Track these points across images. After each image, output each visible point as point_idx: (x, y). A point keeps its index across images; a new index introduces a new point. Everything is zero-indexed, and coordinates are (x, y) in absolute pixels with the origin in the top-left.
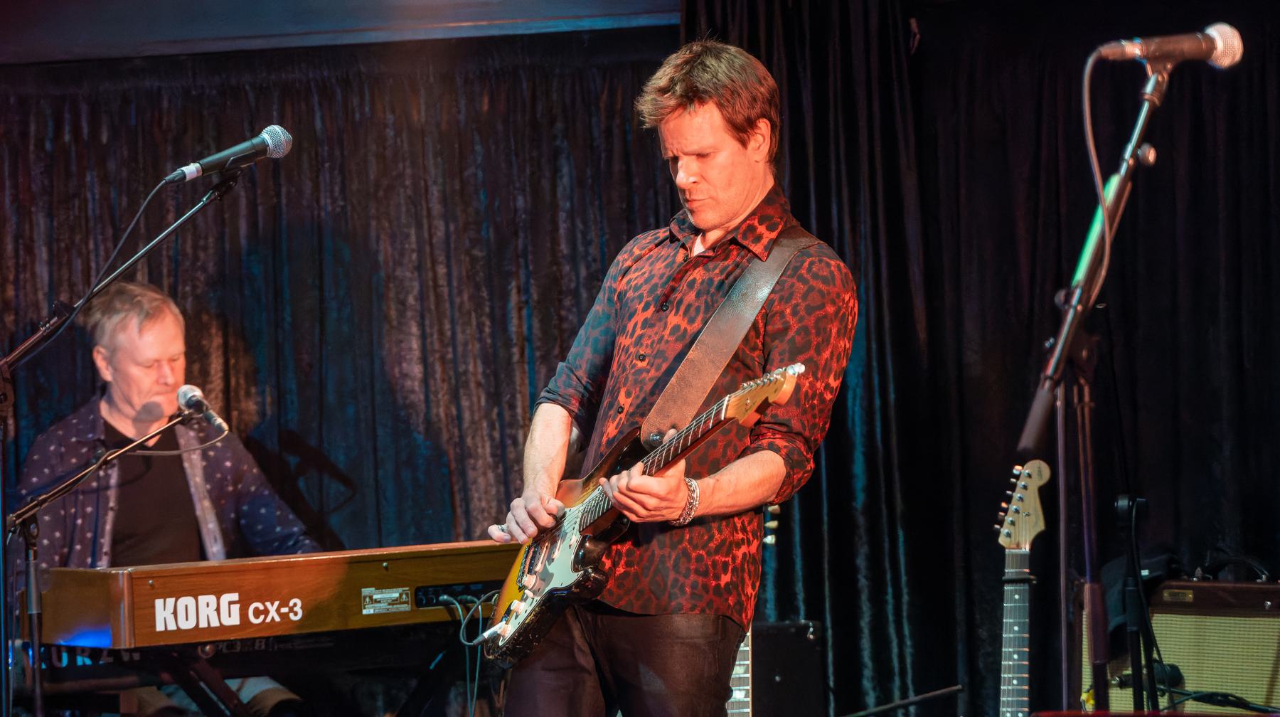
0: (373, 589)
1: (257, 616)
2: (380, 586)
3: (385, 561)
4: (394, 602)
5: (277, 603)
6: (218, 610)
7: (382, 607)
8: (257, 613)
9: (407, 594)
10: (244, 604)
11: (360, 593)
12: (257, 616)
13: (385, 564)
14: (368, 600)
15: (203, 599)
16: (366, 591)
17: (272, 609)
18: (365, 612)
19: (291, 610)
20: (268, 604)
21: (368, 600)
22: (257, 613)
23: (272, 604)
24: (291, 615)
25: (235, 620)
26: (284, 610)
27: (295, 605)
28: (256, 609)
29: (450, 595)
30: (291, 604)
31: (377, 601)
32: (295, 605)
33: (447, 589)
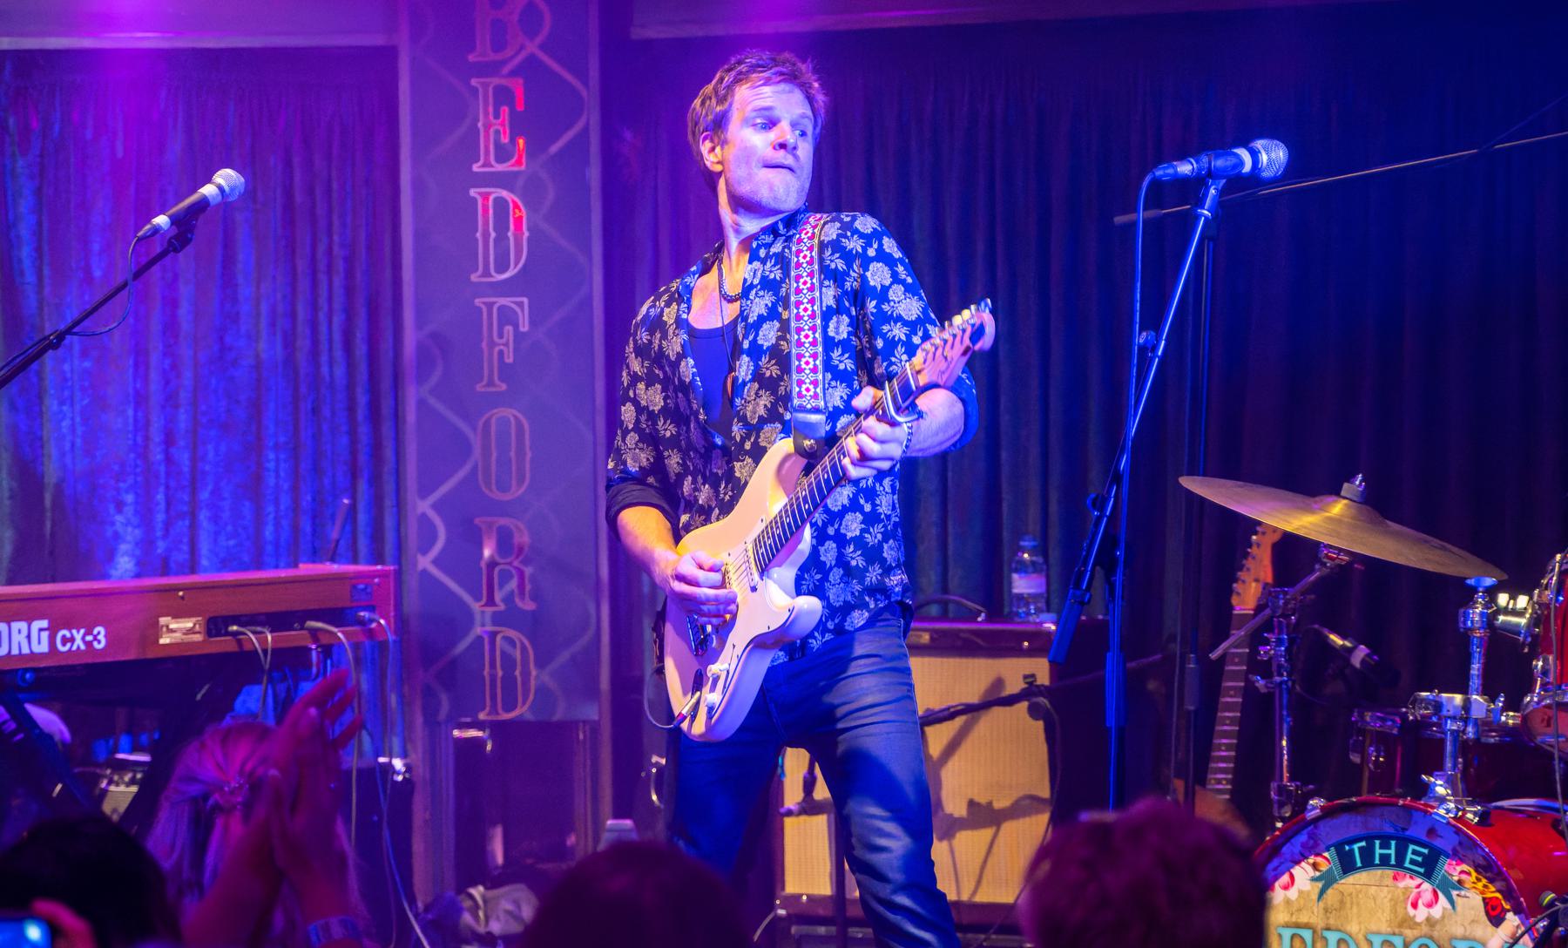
0: (169, 618)
1: (64, 644)
2: (177, 615)
3: (181, 590)
4: (190, 631)
5: (82, 631)
6: (29, 637)
7: (178, 636)
8: (65, 641)
9: (200, 624)
11: (158, 622)
12: (64, 644)
13: (181, 593)
14: (164, 629)
15: (16, 626)
16: (163, 620)
17: (78, 635)
18: (162, 641)
19: (95, 638)
20: (74, 632)
21: (164, 629)
22: (65, 641)
23: (78, 632)
24: (95, 644)
25: (44, 648)
26: (89, 638)
27: (99, 633)
28: (64, 636)
29: (239, 625)
30: (95, 632)
31: (172, 631)
32: (99, 633)
33: (236, 620)
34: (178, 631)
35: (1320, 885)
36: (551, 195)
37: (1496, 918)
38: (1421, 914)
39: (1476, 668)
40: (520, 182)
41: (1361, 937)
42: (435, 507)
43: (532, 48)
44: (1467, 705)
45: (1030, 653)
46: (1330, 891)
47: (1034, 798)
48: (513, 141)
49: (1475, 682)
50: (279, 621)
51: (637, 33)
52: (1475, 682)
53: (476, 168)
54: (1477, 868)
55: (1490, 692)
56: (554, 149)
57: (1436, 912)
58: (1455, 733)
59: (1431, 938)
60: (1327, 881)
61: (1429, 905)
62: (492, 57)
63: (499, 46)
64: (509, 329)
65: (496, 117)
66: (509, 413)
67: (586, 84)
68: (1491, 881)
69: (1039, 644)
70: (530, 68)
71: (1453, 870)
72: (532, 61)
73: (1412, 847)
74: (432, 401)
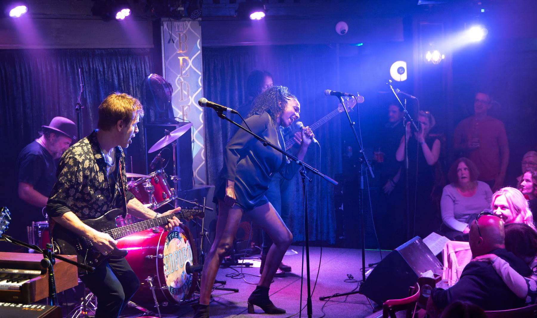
35: (167, 245)
37: (186, 242)
38: (178, 246)
41: (173, 254)
46: (169, 246)
54: (183, 233)
57: (180, 244)
59: (180, 250)
60: (168, 244)
61: (179, 243)
71: (181, 235)
73: (176, 233)
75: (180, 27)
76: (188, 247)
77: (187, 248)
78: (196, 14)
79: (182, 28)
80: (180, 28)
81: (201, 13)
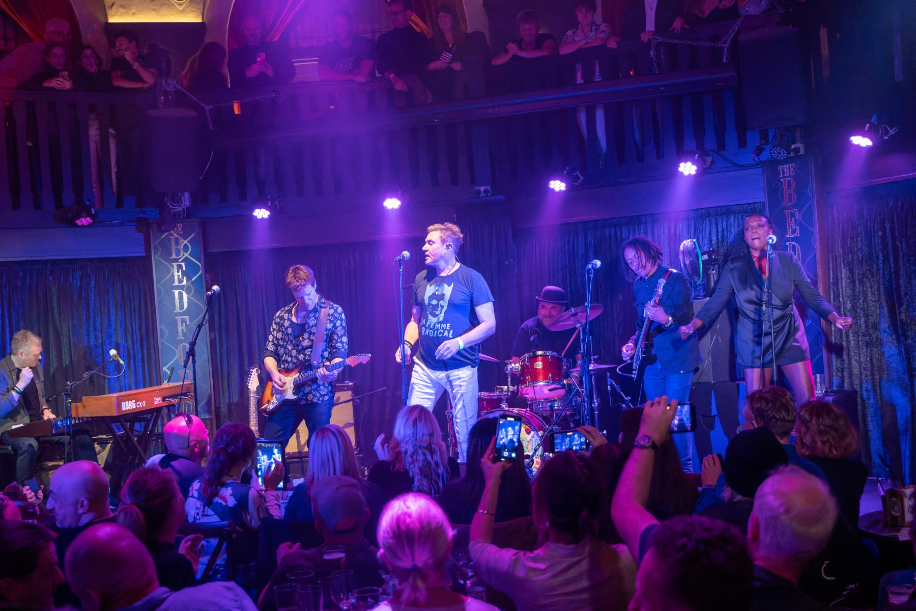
4: (160, 401)
8: (139, 405)
10: (136, 402)
16: (155, 398)
18: (155, 403)
22: (139, 405)
33: (168, 397)
34: (158, 401)
36: (193, 291)
39: (509, 380)
40: (185, 289)
42: (167, 368)
43: (187, 255)
44: (508, 388)
45: (347, 390)
47: (348, 423)
48: (183, 278)
49: (509, 383)
50: (175, 396)
51: (211, 250)
52: (509, 383)
53: (174, 285)
55: (513, 385)
56: (193, 279)
58: (507, 395)
62: (176, 257)
63: (178, 254)
64: (184, 324)
65: (178, 272)
66: (185, 344)
67: (201, 264)
68: (526, 425)
69: (348, 388)
70: (186, 260)
72: (187, 257)
74: (165, 342)
75: (786, 170)
76: (533, 439)
77: (531, 440)
78: (779, 153)
79: (788, 173)
80: (786, 173)
81: (771, 153)
